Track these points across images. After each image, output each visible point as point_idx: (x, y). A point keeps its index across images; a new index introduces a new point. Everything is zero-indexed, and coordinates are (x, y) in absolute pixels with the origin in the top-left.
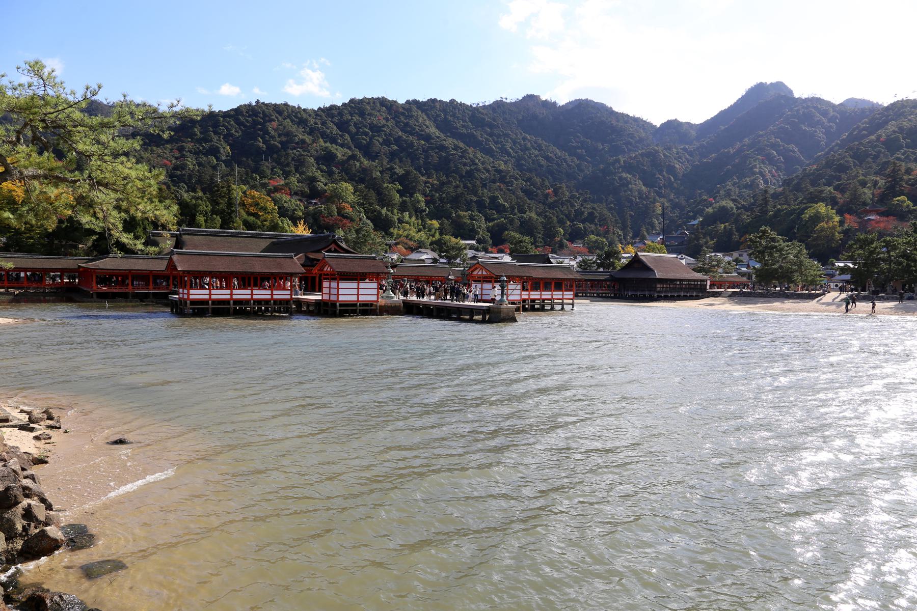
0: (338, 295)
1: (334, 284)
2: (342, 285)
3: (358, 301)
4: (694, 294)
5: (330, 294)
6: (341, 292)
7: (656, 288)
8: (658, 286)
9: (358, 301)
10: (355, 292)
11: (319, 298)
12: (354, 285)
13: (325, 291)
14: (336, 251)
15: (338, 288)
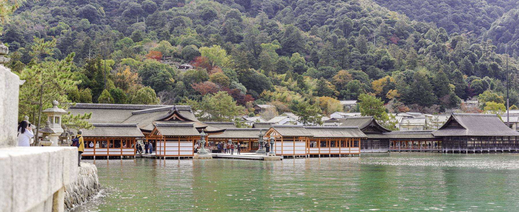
0: (165, 151)
1: (163, 144)
2: (168, 144)
3: (179, 155)
4: (510, 149)
5: (160, 151)
6: (167, 149)
7: (467, 144)
8: (469, 142)
9: (179, 155)
10: (177, 149)
11: (155, 154)
12: (176, 144)
13: (158, 149)
14: (177, 120)
15: (165, 147)
